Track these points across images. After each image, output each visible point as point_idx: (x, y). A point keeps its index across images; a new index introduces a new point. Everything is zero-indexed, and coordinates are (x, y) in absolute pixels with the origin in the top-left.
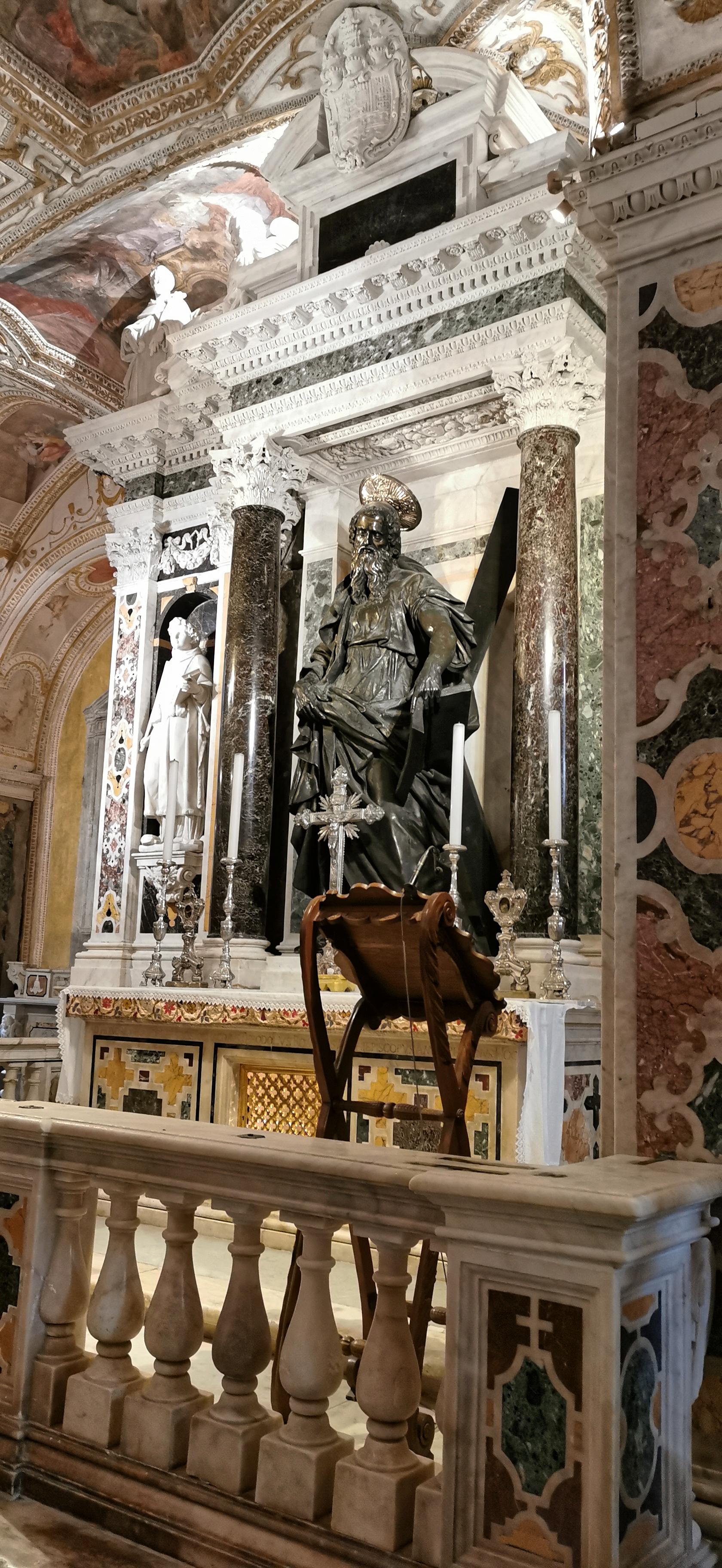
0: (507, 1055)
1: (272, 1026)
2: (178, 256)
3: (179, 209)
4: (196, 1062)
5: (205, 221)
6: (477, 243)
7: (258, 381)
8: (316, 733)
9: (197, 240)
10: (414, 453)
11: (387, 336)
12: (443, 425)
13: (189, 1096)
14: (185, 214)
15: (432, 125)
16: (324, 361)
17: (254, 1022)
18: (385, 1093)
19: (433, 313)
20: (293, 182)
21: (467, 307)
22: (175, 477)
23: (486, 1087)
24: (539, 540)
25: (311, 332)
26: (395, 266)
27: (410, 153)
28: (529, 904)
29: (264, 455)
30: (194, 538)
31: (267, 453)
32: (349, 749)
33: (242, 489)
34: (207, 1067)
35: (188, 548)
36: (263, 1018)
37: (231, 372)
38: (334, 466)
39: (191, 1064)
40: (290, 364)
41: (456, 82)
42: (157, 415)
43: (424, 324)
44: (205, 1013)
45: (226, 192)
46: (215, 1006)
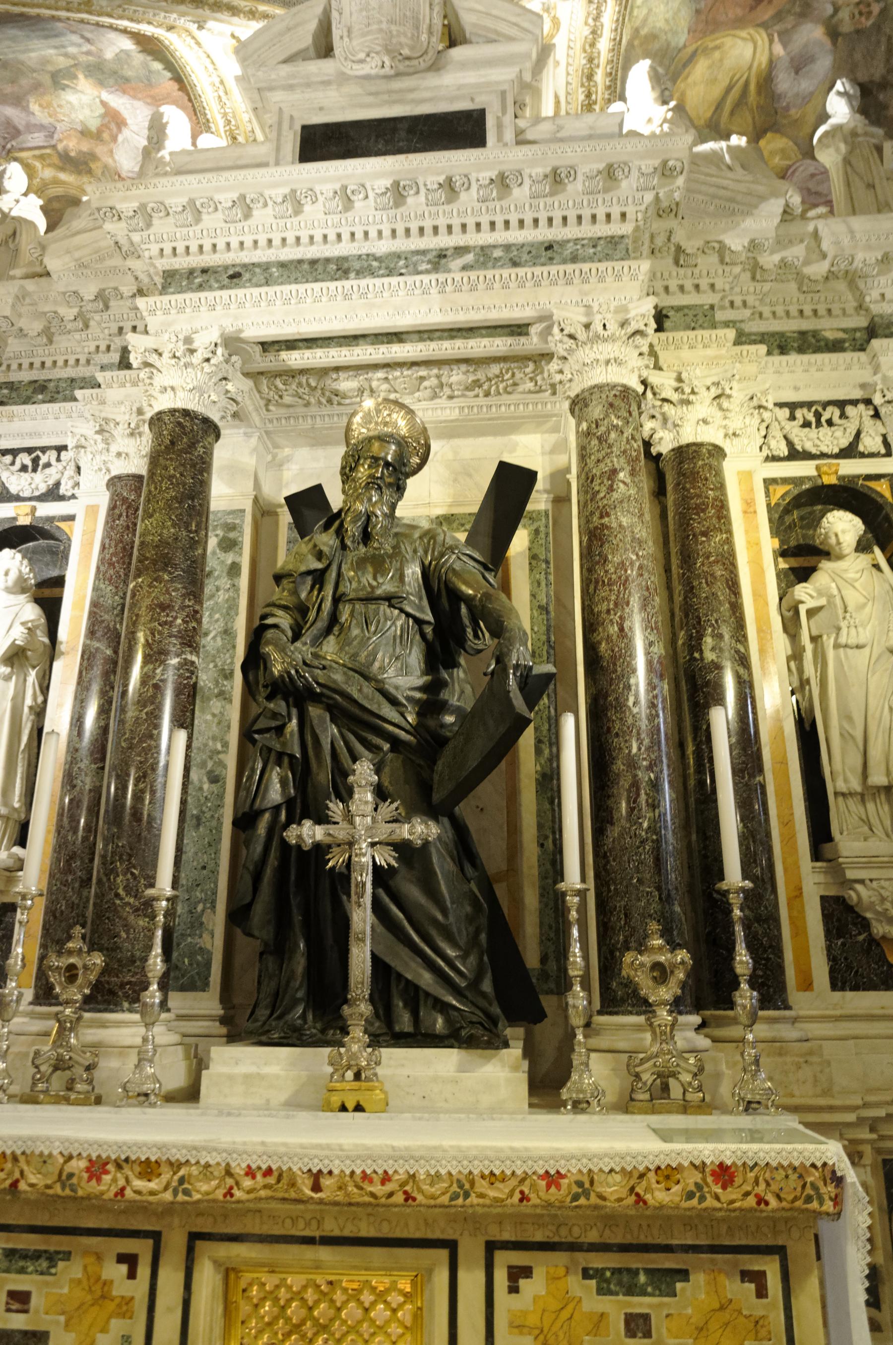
0: (795, 1233)
1: (336, 1204)
2: (42, 157)
3: (69, 97)
4: (144, 1271)
5: (94, 124)
6: (546, 176)
7: (204, 271)
8: (294, 711)
9: (73, 145)
12: (422, 379)
14: (72, 107)
15: (464, 65)
16: (306, 266)
17: (293, 1195)
18: (565, 1314)
19: (462, 244)
20: (273, 77)
21: (507, 247)
23: (762, 1292)
26: (439, 174)
27: (427, 89)
28: (694, 973)
29: (214, 353)
30: (35, 461)
31: (220, 351)
32: (351, 738)
33: (173, 388)
34: (170, 1280)
35: (24, 468)
36: (316, 1188)
37: (168, 251)
38: (262, 403)
39: (132, 1275)
41: (496, 32)
42: (10, 301)
43: (449, 253)
44: (182, 1181)
45: (134, 97)
46: (207, 1166)
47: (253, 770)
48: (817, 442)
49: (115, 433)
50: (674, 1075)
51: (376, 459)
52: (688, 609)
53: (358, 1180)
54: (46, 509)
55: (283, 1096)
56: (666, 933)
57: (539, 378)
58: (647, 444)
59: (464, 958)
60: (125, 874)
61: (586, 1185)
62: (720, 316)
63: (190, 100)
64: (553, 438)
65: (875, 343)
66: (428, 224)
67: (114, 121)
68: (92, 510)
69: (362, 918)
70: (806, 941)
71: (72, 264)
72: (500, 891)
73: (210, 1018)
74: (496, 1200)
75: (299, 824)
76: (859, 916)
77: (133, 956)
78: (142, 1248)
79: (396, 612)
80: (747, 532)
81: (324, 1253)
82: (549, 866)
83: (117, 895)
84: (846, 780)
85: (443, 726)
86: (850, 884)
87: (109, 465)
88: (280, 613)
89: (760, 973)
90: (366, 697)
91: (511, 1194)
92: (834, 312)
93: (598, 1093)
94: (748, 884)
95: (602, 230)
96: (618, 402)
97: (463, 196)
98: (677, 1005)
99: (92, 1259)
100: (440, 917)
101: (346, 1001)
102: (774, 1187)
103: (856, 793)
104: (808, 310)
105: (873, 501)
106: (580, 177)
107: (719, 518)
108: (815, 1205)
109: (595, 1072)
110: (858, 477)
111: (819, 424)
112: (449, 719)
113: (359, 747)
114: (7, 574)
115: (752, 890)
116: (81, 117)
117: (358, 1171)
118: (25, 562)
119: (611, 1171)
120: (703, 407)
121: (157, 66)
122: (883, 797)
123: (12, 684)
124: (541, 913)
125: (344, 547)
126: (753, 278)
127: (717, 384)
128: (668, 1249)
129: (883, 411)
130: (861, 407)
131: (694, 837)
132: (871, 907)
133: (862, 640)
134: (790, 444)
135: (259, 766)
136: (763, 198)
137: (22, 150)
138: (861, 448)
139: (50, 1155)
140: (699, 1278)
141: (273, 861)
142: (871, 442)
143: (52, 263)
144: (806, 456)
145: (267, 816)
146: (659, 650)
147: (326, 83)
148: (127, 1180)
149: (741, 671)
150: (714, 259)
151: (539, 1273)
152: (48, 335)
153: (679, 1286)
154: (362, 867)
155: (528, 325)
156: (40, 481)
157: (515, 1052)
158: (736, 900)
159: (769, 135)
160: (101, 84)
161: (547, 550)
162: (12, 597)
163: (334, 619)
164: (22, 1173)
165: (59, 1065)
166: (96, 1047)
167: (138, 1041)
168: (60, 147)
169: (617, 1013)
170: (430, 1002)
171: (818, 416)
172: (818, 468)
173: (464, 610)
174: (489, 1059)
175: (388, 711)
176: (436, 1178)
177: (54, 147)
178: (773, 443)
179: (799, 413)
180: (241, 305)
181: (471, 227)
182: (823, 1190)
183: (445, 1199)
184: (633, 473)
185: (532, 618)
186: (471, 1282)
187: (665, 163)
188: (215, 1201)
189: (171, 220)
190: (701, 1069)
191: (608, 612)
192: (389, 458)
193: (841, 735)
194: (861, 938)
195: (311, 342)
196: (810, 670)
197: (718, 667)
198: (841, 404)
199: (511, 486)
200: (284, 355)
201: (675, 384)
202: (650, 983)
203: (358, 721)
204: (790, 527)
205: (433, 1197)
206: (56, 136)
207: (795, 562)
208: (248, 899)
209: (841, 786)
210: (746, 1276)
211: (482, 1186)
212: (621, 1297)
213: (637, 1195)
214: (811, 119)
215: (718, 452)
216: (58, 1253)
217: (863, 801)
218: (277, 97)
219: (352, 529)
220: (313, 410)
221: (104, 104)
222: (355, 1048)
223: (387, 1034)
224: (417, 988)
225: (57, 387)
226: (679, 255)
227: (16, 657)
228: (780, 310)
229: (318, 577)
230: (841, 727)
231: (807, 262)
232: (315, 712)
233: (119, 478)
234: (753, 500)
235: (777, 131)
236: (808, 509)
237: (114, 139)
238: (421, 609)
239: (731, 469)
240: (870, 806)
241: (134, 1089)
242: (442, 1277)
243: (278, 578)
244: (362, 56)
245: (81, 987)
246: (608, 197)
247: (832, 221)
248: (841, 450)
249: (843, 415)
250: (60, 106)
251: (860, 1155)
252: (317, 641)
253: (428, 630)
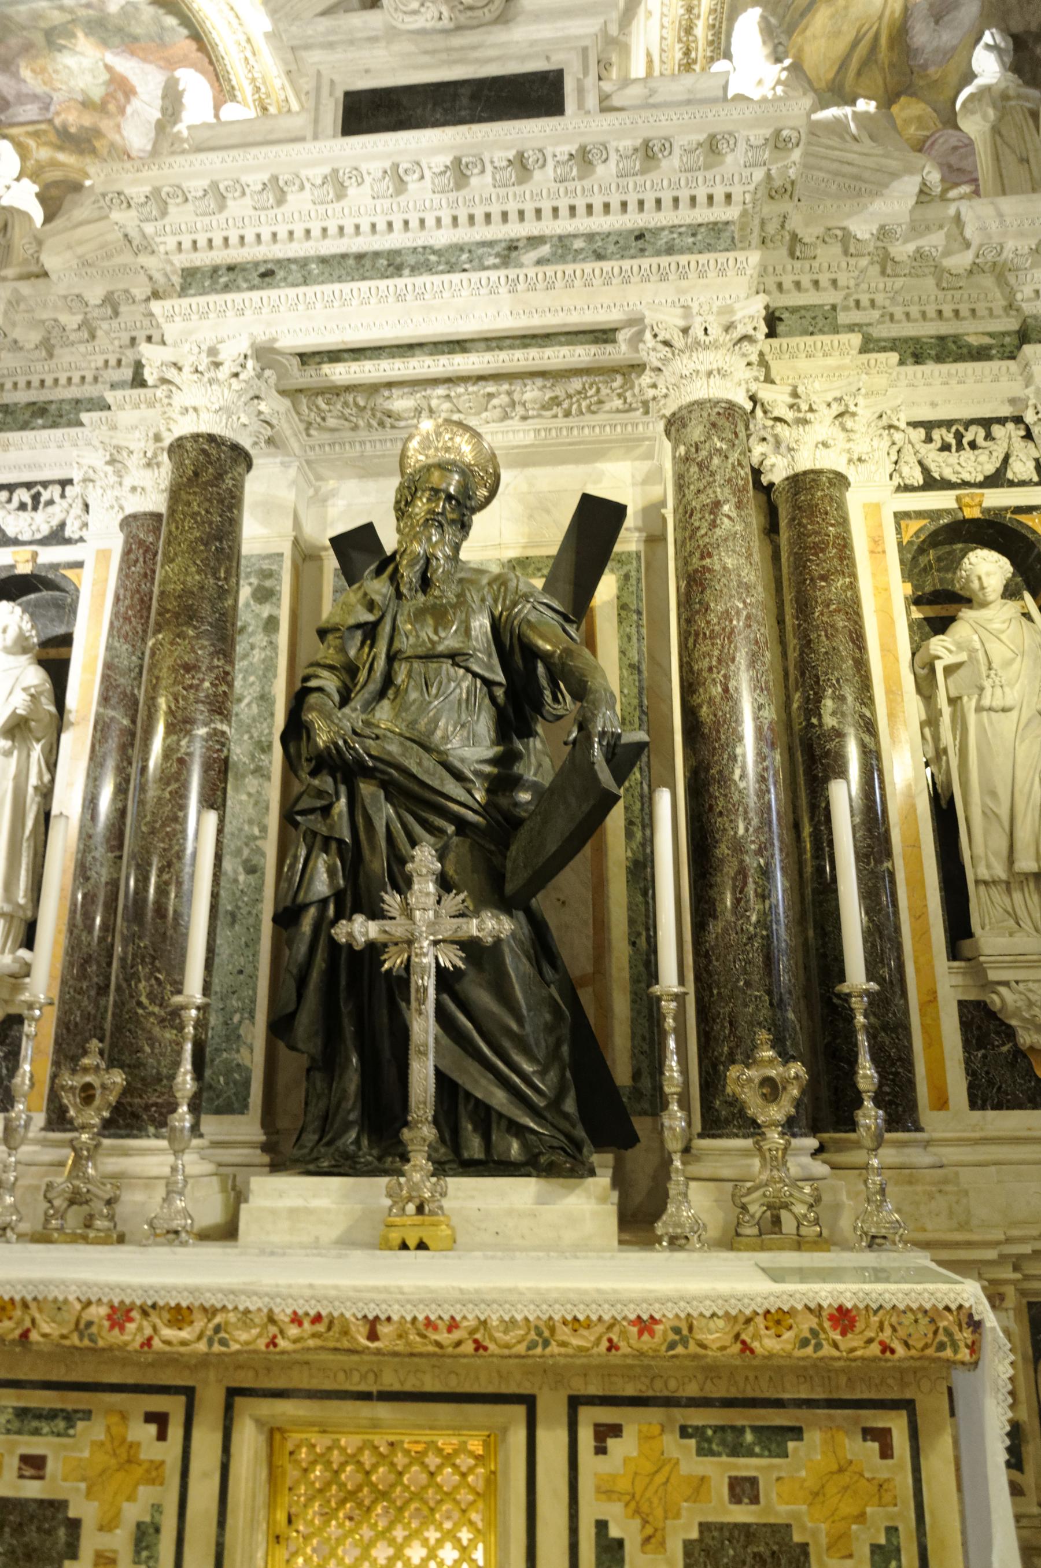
0: (926, 1385)
1: (396, 1354)
2: (36, 134)
3: (67, 60)
4: (175, 1431)
5: (97, 93)
6: (636, 150)
7: (231, 268)
8: (343, 789)
9: (74, 119)
11: (460, 248)
12: (490, 396)
13: (157, 1508)
16: (351, 262)
17: (346, 1344)
18: (660, 1479)
19: (536, 233)
20: (310, 32)
21: (590, 237)
23: (886, 1453)
24: (730, 543)
25: (336, 215)
26: (508, 148)
27: (493, 46)
28: (811, 1089)
29: (243, 366)
30: (36, 498)
31: (250, 363)
32: (410, 819)
33: (195, 409)
35: (22, 507)
36: (373, 1336)
37: (187, 245)
38: (302, 426)
39: (162, 1436)
40: (291, 255)
43: (521, 244)
44: (217, 1329)
45: (145, 60)
46: (247, 1312)
47: (296, 858)
48: (958, 468)
49: (129, 463)
50: (786, 1206)
51: (436, 491)
52: (804, 667)
53: (421, 1327)
54: (50, 555)
55: (335, 1232)
56: (778, 1044)
57: (628, 394)
58: (757, 472)
59: (543, 1073)
60: (148, 980)
61: (684, 1331)
62: (843, 318)
63: (211, 63)
64: (645, 466)
65: (1027, 349)
66: (495, 210)
67: (121, 89)
68: (104, 555)
69: (423, 1028)
70: (941, 1052)
71: (74, 263)
72: (585, 996)
73: (250, 1145)
74: (580, 1349)
75: (350, 919)
77: (159, 1073)
78: (174, 1406)
79: (461, 671)
80: (874, 575)
81: (383, 1411)
82: (642, 969)
83: (139, 1004)
84: (989, 866)
85: (516, 804)
86: (991, 986)
87: (123, 502)
88: (325, 673)
89: (887, 1089)
90: (426, 771)
91: (597, 1342)
92: (979, 313)
93: (698, 1227)
94: (873, 986)
95: (703, 215)
96: (721, 422)
97: (537, 175)
98: (790, 1127)
99: (115, 1419)
100: (514, 1026)
101: (406, 1124)
102: (902, 1333)
103: (1001, 881)
104: (947, 310)
105: (1024, 538)
106: (677, 151)
107: (841, 559)
108: (948, 1353)
109: (695, 1203)
110: (1006, 509)
111: (960, 447)
112: (525, 797)
113: (418, 830)
114: (4, 631)
115: (878, 993)
116: (82, 85)
117: (421, 1317)
118: (26, 617)
119: (714, 1315)
120: (823, 426)
121: (171, 21)
122: (1032, 885)
123: (13, 760)
124: (634, 1021)
125: (399, 595)
126: (883, 273)
127: (840, 400)
128: (778, 1404)
129: (1035, 431)
130: (1010, 426)
131: (811, 933)
132: (1017, 1013)
133: (1009, 702)
134: (925, 470)
135: (303, 852)
136: (895, 175)
137: (12, 125)
138: (1010, 475)
139: (66, 1301)
140: (814, 1437)
141: (320, 963)
142: (1022, 468)
143: (50, 261)
144: (946, 485)
145: (312, 911)
146: (769, 714)
147: (373, 40)
148: (155, 1329)
149: (867, 739)
150: (837, 249)
151: (630, 1432)
152: (48, 347)
153: (791, 1445)
154: (424, 969)
155: (615, 330)
156: (42, 522)
157: (602, 1181)
158: (859, 1005)
159: (903, 99)
160: (105, 43)
161: (639, 598)
162: (11, 658)
163: (388, 680)
164: (33, 1321)
165: (75, 1199)
166: (118, 1178)
167: (166, 1171)
168: (57, 121)
169: (720, 1136)
170: (504, 1124)
171: (959, 436)
172: (958, 499)
173: (541, 669)
174: (572, 1189)
175: (452, 788)
176: (511, 1324)
177: (50, 121)
178: (905, 470)
179: (936, 434)
180: (275, 309)
181: (547, 213)
182: (958, 1336)
183: (521, 1349)
184: (739, 506)
185: (621, 679)
186: (552, 1442)
187: (778, 133)
188: (256, 1352)
189: (189, 207)
190: (818, 1200)
191: (710, 669)
192: (452, 490)
193: (984, 813)
194: (1005, 1049)
195: (358, 353)
197: (839, 734)
198: (986, 423)
200: (327, 368)
202: (759, 1101)
203: (416, 799)
204: (925, 569)
205: (507, 1346)
206: (52, 109)
207: (931, 611)
208: (291, 1008)
209: (984, 873)
210: (869, 1433)
211: (564, 1333)
212: (724, 1459)
213: (744, 1342)
214: (953, 79)
215: (840, 480)
216: (76, 1411)
218: (315, 57)
219: (409, 574)
220: (363, 434)
221: (108, 68)
222: (417, 1177)
223: (454, 1161)
224: (488, 1108)
225: (60, 410)
226: (795, 245)
227: (18, 728)
228: (914, 310)
229: (370, 631)
230: (984, 805)
231: (947, 253)
232: (367, 789)
233: (134, 517)
234: (881, 537)
235: (914, 95)
237: (122, 111)
238: (490, 668)
239: (855, 501)
240: (1017, 896)
241: (162, 1226)
242: (518, 1437)
243: (323, 633)
244: (415, 5)
245: (99, 1110)
246: (709, 175)
247: (976, 202)
248: (986, 478)
249: (989, 436)
250: (56, 71)
251: (1002, 1297)
252: (369, 706)
253: (499, 692)
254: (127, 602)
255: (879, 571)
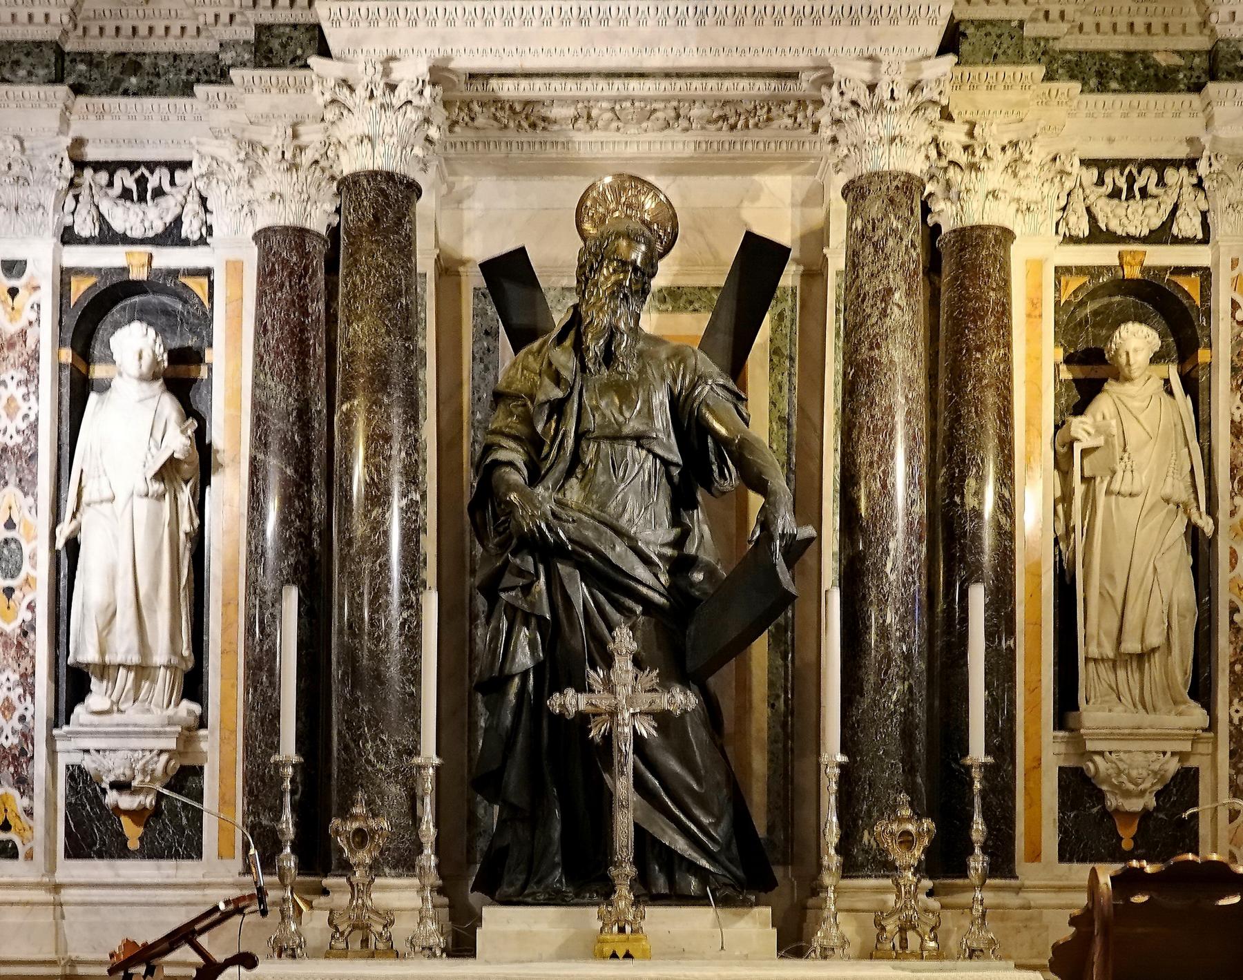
10: (578, 137)
22: (89, 58)
30: (142, 182)
48: (1125, 221)
49: (263, 164)
52: (952, 442)
58: (926, 210)
64: (808, 181)
65: (1212, 88)
68: (235, 268)
69: (623, 787)
70: (1039, 809)
76: (1095, 787)
83: (368, 762)
85: (692, 584)
87: (255, 206)
89: (990, 843)
92: (1171, 30)
94: (990, 760)
100: (695, 787)
103: (1108, 659)
110: (1166, 269)
111: (1131, 196)
112: (698, 577)
115: (992, 766)
120: (993, 176)
122: (1135, 665)
127: (1015, 145)
129: (1206, 185)
130: (1184, 171)
133: (1136, 489)
134: (1093, 219)
135: (505, 625)
142: (1188, 225)
144: (1110, 238)
145: (517, 680)
149: (1003, 520)
158: (976, 774)
169: (857, 877)
171: (1131, 180)
172: (1120, 256)
174: (741, 916)
178: (1072, 219)
194: (1095, 810)
196: (1077, 519)
198: (1160, 165)
199: (759, 260)
201: (965, 140)
204: (1080, 323)
209: (1094, 651)
215: (1006, 236)
217: (1114, 668)
220: (511, 134)
222: (622, 904)
223: (647, 895)
225: (156, 66)
230: (1101, 586)
234: (1040, 300)
236: (1105, 300)
239: (1018, 255)
240: (1121, 673)
243: (499, 397)
249: (1161, 182)
254: (277, 334)
255: (1034, 338)
